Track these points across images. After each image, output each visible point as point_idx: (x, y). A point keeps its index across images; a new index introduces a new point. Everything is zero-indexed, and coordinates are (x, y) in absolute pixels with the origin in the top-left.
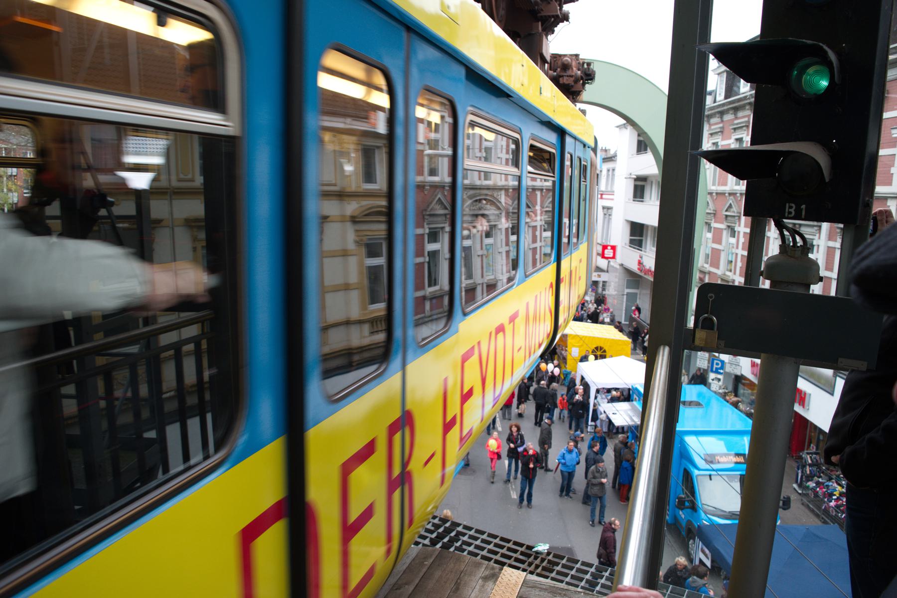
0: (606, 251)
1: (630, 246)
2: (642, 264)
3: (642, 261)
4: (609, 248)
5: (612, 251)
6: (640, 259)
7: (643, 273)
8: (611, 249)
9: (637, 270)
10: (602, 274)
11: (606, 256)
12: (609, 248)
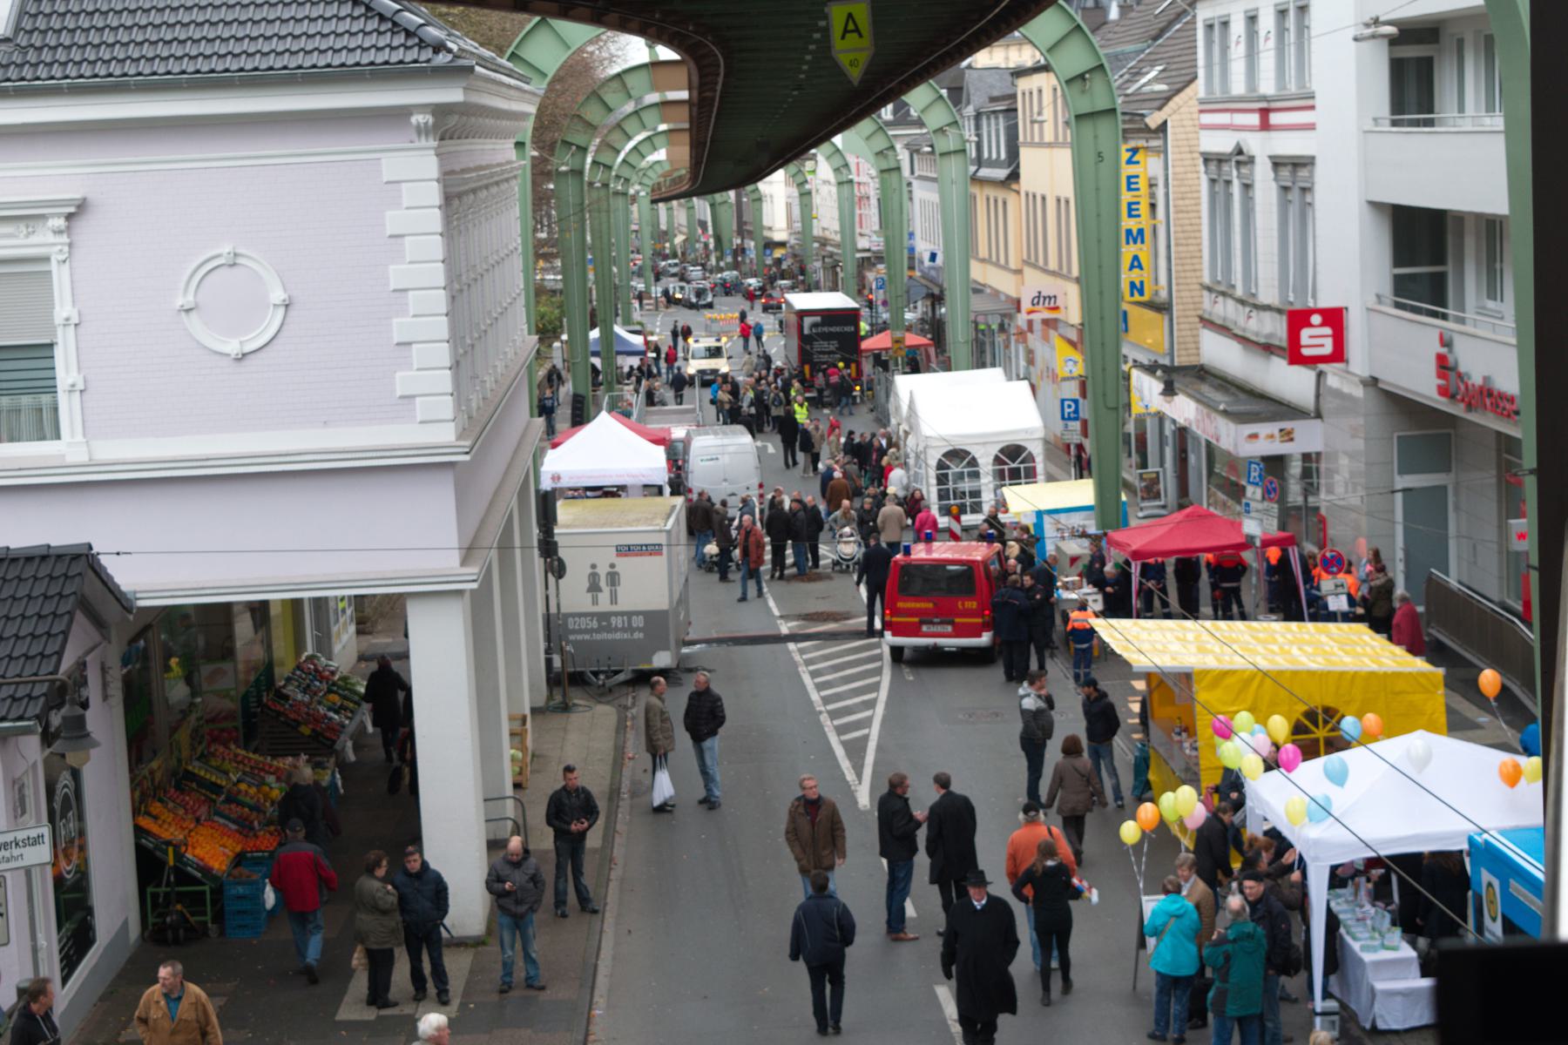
0: (1305, 334)
1: (1398, 306)
2: (1454, 369)
3: (1451, 359)
4: (1316, 319)
5: (1328, 331)
6: (1444, 350)
7: (1462, 405)
8: (1323, 324)
9: (1434, 394)
10: (1297, 426)
11: (1306, 352)
12: (1316, 319)
